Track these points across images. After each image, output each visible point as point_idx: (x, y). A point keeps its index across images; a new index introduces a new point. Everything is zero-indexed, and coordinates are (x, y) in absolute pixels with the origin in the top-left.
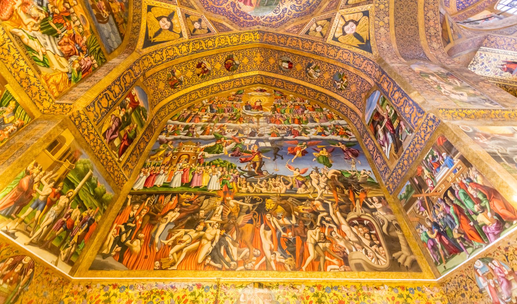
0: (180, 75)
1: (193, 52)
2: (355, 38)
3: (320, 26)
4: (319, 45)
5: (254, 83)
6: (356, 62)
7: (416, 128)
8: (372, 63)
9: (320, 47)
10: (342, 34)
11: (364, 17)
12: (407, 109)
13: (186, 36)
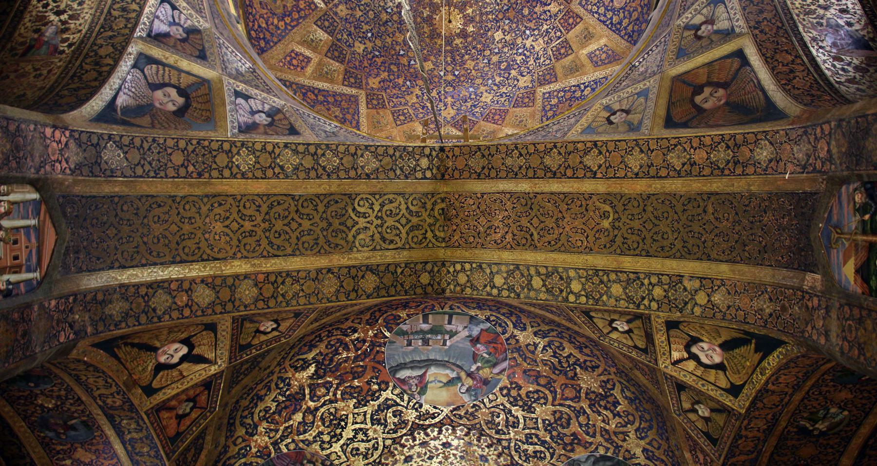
2: (737, 351)
3: (696, 407)
4: (749, 424)
10: (720, 372)
11: (681, 327)
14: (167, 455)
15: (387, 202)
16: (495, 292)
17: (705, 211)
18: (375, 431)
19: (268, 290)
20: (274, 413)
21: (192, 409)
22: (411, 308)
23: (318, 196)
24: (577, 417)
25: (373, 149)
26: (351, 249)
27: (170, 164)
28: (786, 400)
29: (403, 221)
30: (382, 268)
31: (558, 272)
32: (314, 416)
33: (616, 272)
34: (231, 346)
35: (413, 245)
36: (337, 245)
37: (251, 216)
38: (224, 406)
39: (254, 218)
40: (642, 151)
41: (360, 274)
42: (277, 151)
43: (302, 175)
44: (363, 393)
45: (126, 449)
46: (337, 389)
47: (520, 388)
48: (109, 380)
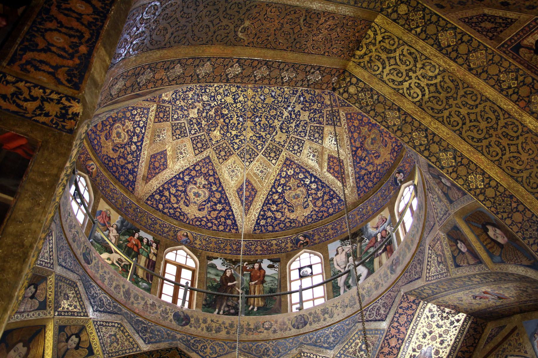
7: (16, 68)
12: (59, 40)
15: (396, 83)
17: (172, 34)
19: (524, 91)
23: (442, 123)
25: (384, 123)
26: (444, 71)
27: (525, 219)
29: (392, 61)
30: (431, 41)
35: (396, 40)
36: (452, 81)
37: (498, 146)
39: (497, 143)
40: (198, 75)
41: (449, 50)
42: (450, 170)
43: (443, 144)
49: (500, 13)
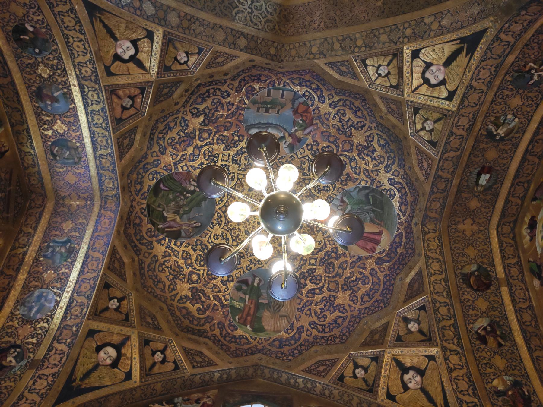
0: (504, 382)
1: (459, 344)
2: (454, 63)
3: (425, 125)
5: (514, 239)
6: (499, 52)
8: (507, 25)
9: (462, 119)
10: (443, 87)
13: (433, 351)
14: (113, 129)
16: (312, 56)
18: (234, 167)
19: (186, 24)
20: (177, 143)
21: (132, 106)
22: (261, 82)
24: (350, 163)
26: (234, 20)
28: (482, 99)
29: (264, 15)
30: (250, 37)
31: (349, 37)
32: (200, 151)
33: (384, 28)
34: (160, 62)
36: (226, 15)
38: (150, 116)
44: (229, 141)
45: (88, 119)
46: (214, 135)
47: (318, 144)
48: (87, 46)
49: (214, 70)
